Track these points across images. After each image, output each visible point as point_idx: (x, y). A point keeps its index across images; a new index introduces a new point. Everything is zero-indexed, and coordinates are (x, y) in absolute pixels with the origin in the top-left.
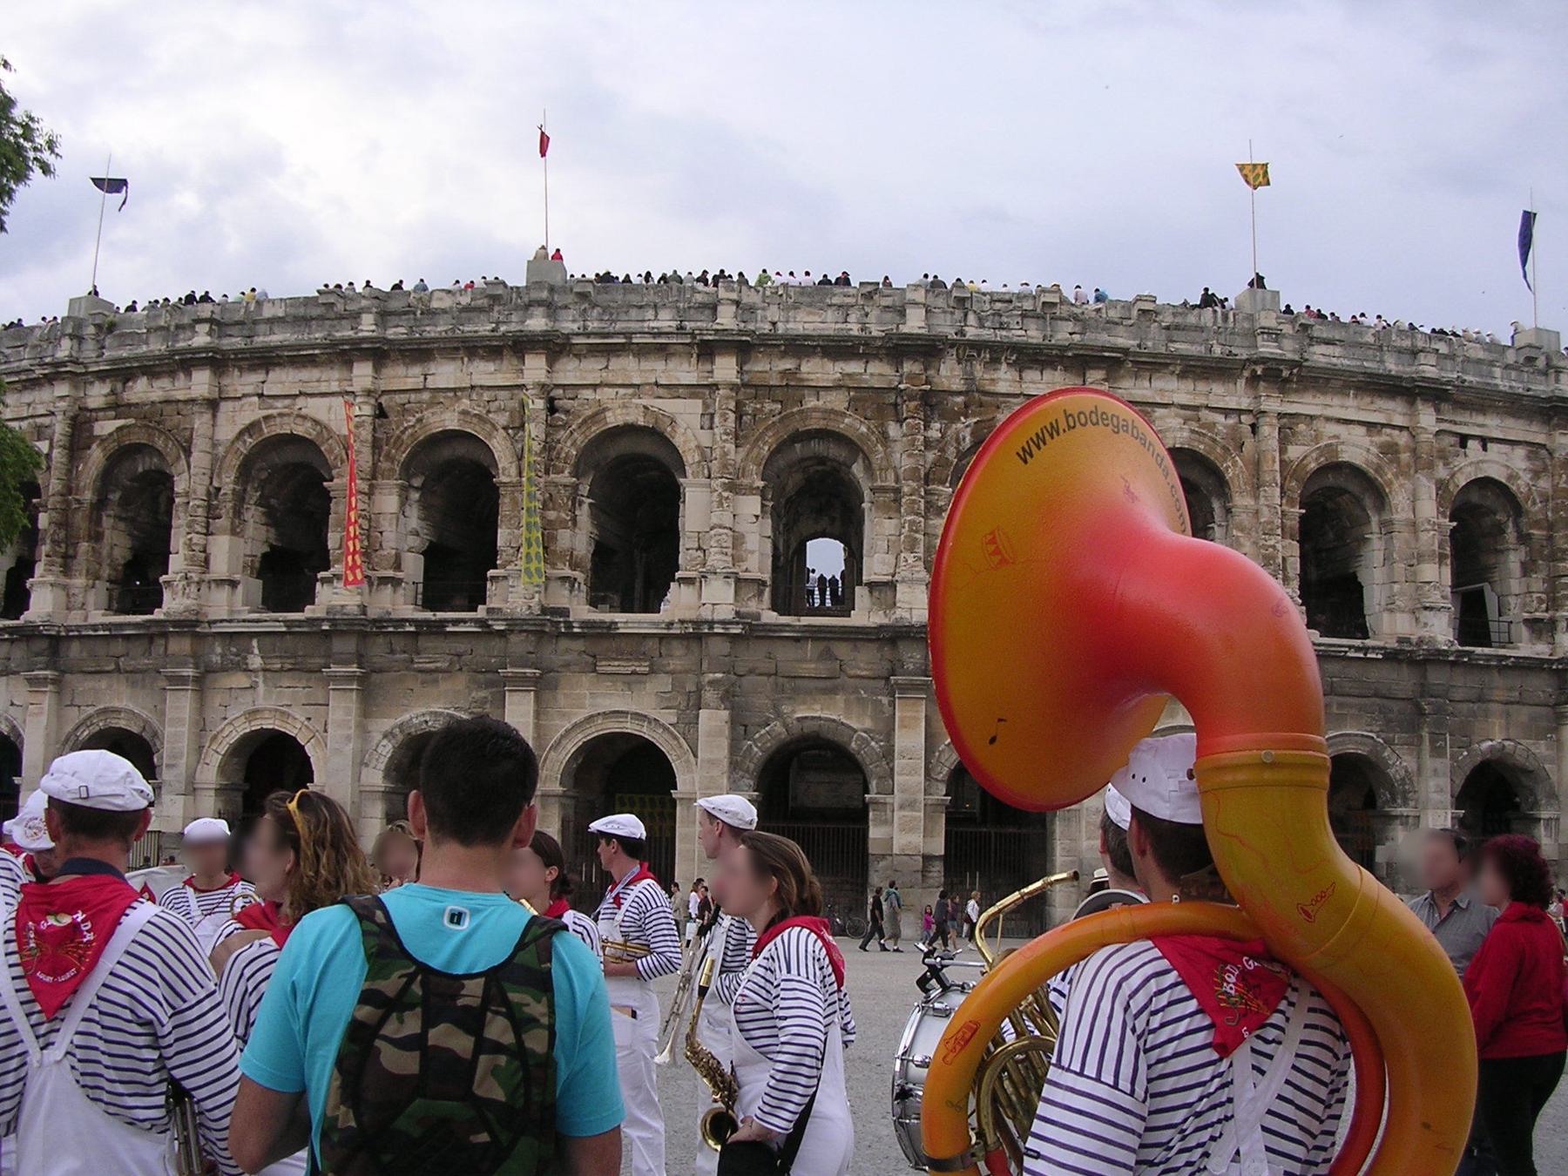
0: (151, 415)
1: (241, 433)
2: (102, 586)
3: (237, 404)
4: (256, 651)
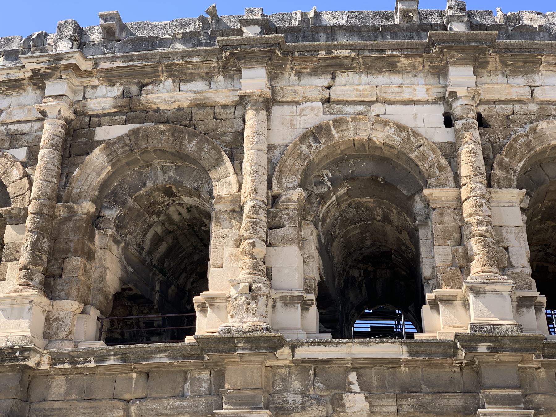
0: (181, 121)
1: (304, 138)
2: (94, 313)
3: (295, 109)
4: (355, 388)
